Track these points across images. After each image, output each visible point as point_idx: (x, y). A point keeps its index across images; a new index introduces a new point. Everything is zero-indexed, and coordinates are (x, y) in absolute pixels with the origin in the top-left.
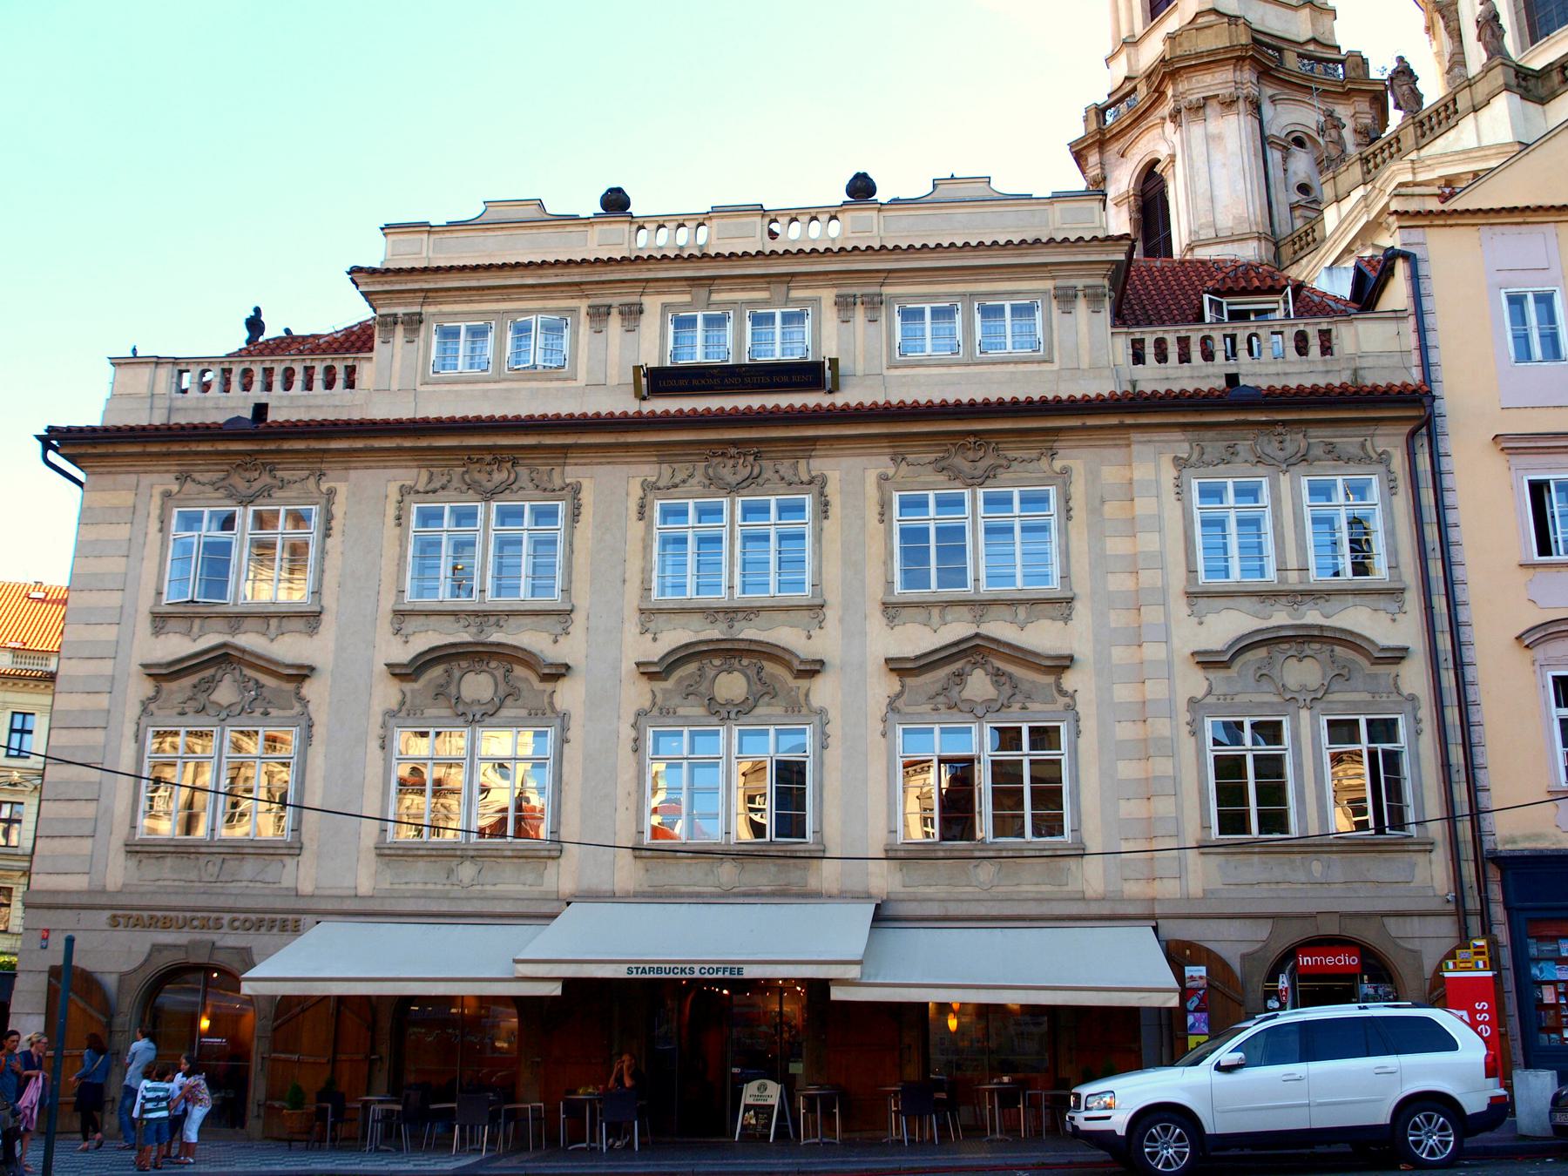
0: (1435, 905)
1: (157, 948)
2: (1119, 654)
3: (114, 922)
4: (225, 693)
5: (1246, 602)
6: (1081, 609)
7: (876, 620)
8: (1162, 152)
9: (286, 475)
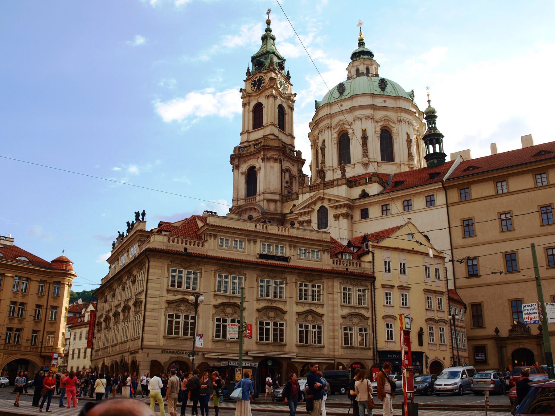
0: (371, 358)
1: (171, 358)
2: (330, 314)
3: (162, 352)
4: (182, 308)
5: (349, 308)
6: (325, 306)
7: (295, 305)
8: (257, 166)
9: (193, 264)
